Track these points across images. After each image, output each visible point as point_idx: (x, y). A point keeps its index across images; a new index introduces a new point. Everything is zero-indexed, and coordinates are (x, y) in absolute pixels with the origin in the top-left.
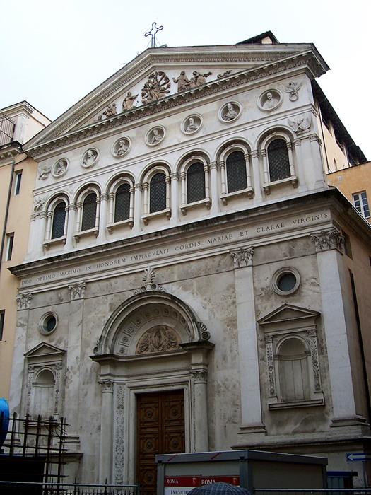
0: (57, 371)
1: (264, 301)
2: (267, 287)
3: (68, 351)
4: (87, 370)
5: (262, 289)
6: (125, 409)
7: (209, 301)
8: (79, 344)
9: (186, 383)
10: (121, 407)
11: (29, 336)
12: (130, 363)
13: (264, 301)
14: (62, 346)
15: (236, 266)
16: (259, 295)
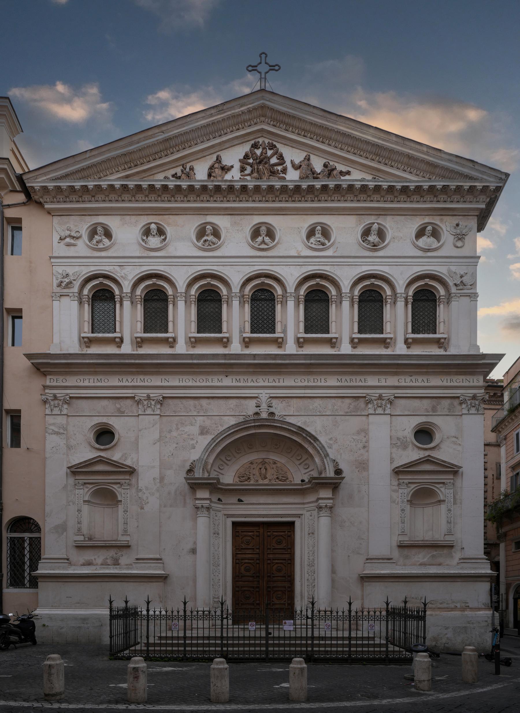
0: (123, 491)
1: (400, 450)
2: (404, 438)
3: (140, 470)
4: (169, 493)
5: (398, 439)
6: (221, 536)
7: (336, 441)
8: (157, 463)
9: (299, 516)
10: (216, 533)
11: (69, 447)
12: (229, 491)
13: (400, 450)
14: (128, 462)
15: (371, 411)
16: (394, 444)
